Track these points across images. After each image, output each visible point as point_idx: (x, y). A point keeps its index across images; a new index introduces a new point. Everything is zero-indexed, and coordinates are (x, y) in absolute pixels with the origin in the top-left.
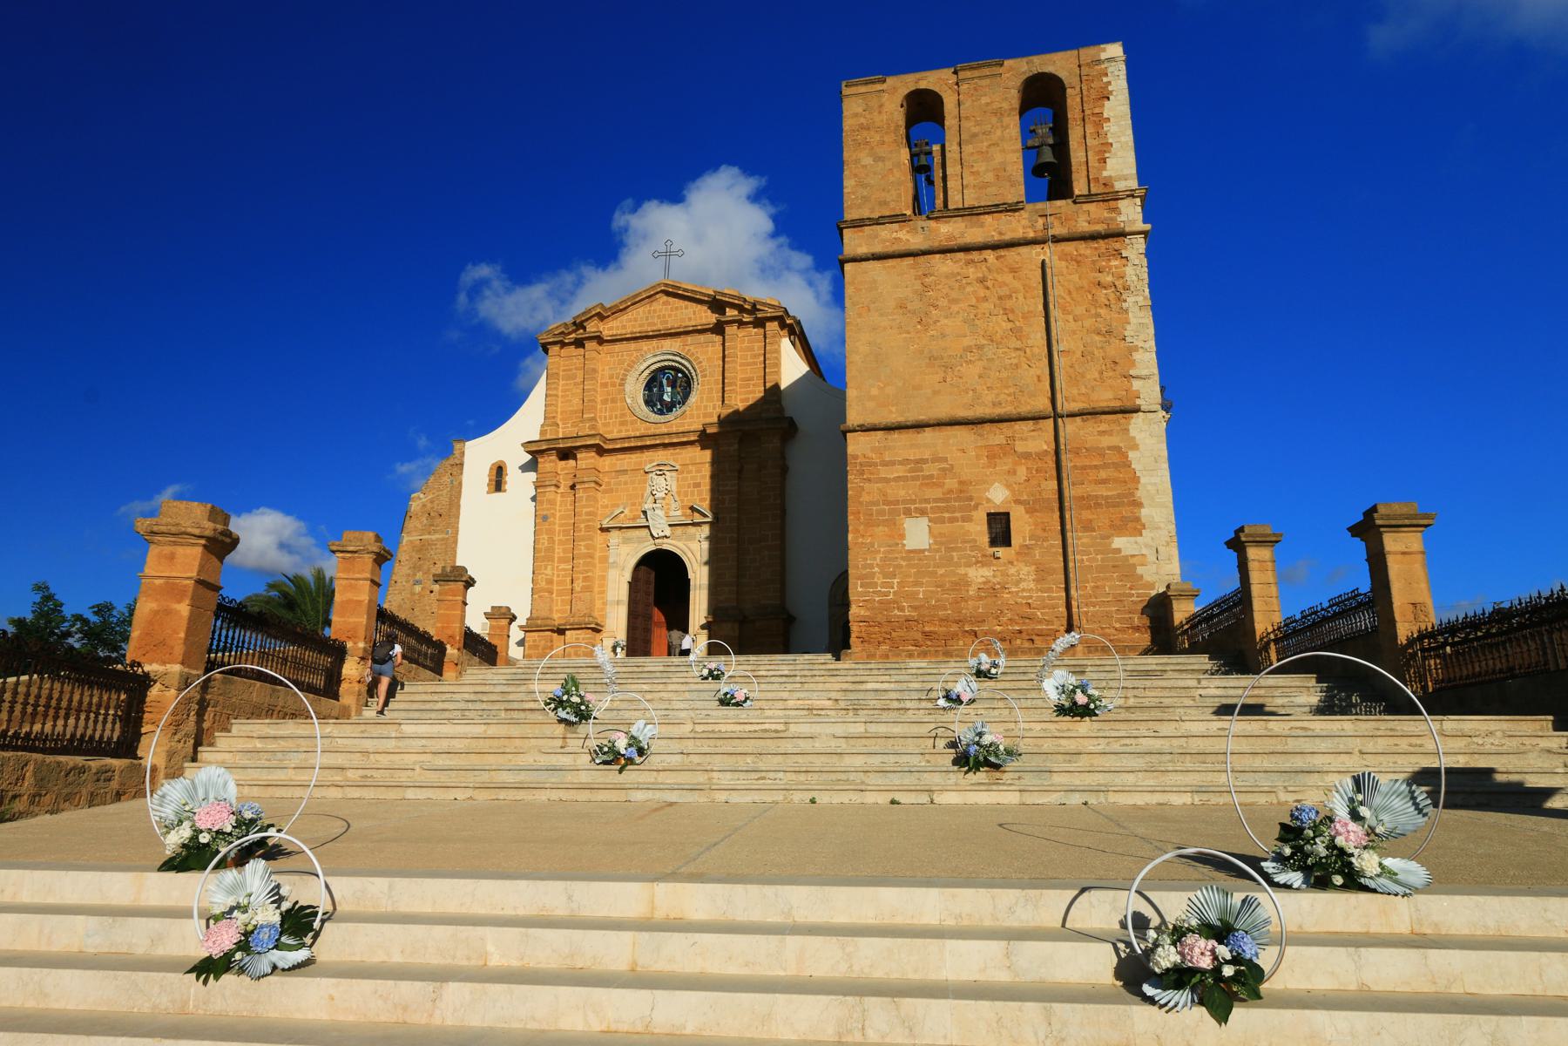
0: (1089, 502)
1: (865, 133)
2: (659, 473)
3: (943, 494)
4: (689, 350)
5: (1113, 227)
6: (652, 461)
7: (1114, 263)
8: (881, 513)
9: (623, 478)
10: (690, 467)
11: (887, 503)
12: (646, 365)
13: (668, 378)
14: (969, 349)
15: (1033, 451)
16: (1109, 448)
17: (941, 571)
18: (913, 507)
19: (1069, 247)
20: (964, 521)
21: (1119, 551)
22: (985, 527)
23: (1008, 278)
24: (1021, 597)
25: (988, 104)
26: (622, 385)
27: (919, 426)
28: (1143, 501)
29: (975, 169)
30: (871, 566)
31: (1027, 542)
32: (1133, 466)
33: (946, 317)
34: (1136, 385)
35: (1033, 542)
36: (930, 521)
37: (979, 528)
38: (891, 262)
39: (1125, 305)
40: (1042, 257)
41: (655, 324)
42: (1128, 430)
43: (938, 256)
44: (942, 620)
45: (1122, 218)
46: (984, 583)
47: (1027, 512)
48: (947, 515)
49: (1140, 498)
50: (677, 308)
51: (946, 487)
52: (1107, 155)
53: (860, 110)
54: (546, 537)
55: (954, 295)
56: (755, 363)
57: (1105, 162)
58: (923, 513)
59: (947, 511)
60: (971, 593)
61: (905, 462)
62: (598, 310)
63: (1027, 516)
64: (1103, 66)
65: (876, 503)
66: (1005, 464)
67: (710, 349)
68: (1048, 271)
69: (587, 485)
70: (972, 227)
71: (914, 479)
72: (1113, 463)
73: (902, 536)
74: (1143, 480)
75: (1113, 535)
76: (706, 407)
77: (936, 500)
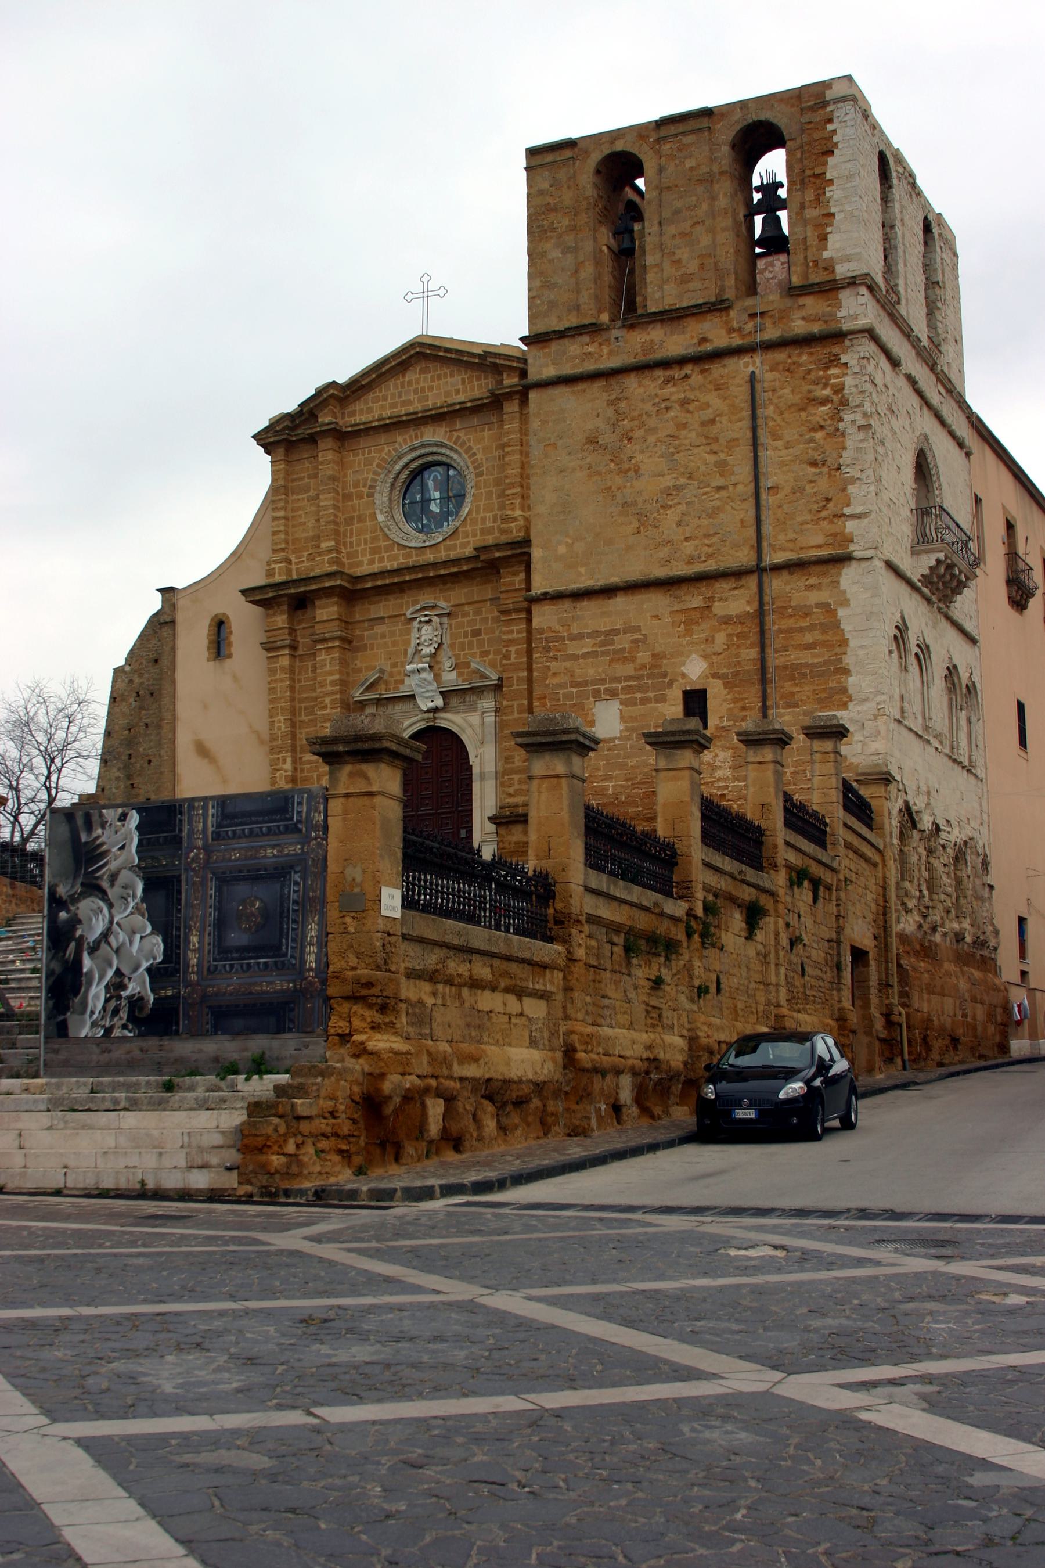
0: (794, 672)
1: (552, 216)
2: (423, 619)
4: (459, 437)
5: (833, 327)
6: (416, 602)
7: (833, 371)
8: (568, 696)
9: (379, 629)
10: (467, 608)
11: (574, 684)
12: (402, 463)
13: (435, 476)
16: (817, 606)
17: (631, 762)
18: (602, 688)
19: (780, 356)
20: (657, 701)
25: (692, 169)
26: (371, 495)
27: (608, 591)
28: (851, 668)
29: (677, 257)
31: (725, 724)
32: (842, 627)
33: (642, 452)
34: (851, 526)
35: (731, 723)
36: (621, 704)
38: (581, 386)
39: (841, 425)
40: (751, 369)
41: (409, 402)
42: (838, 583)
43: (633, 375)
45: (843, 313)
47: (725, 688)
48: (639, 695)
49: (848, 664)
50: (439, 378)
51: (639, 661)
52: (829, 230)
53: (546, 185)
54: (282, 718)
55: (652, 422)
58: (613, 694)
59: (639, 691)
61: (596, 633)
62: (331, 391)
63: (725, 692)
64: (829, 109)
65: (562, 686)
66: (700, 633)
67: (486, 433)
68: (758, 387)
69: (330, 645)
71: (605, 653)
72: (821, 624)
76: (484, 519)
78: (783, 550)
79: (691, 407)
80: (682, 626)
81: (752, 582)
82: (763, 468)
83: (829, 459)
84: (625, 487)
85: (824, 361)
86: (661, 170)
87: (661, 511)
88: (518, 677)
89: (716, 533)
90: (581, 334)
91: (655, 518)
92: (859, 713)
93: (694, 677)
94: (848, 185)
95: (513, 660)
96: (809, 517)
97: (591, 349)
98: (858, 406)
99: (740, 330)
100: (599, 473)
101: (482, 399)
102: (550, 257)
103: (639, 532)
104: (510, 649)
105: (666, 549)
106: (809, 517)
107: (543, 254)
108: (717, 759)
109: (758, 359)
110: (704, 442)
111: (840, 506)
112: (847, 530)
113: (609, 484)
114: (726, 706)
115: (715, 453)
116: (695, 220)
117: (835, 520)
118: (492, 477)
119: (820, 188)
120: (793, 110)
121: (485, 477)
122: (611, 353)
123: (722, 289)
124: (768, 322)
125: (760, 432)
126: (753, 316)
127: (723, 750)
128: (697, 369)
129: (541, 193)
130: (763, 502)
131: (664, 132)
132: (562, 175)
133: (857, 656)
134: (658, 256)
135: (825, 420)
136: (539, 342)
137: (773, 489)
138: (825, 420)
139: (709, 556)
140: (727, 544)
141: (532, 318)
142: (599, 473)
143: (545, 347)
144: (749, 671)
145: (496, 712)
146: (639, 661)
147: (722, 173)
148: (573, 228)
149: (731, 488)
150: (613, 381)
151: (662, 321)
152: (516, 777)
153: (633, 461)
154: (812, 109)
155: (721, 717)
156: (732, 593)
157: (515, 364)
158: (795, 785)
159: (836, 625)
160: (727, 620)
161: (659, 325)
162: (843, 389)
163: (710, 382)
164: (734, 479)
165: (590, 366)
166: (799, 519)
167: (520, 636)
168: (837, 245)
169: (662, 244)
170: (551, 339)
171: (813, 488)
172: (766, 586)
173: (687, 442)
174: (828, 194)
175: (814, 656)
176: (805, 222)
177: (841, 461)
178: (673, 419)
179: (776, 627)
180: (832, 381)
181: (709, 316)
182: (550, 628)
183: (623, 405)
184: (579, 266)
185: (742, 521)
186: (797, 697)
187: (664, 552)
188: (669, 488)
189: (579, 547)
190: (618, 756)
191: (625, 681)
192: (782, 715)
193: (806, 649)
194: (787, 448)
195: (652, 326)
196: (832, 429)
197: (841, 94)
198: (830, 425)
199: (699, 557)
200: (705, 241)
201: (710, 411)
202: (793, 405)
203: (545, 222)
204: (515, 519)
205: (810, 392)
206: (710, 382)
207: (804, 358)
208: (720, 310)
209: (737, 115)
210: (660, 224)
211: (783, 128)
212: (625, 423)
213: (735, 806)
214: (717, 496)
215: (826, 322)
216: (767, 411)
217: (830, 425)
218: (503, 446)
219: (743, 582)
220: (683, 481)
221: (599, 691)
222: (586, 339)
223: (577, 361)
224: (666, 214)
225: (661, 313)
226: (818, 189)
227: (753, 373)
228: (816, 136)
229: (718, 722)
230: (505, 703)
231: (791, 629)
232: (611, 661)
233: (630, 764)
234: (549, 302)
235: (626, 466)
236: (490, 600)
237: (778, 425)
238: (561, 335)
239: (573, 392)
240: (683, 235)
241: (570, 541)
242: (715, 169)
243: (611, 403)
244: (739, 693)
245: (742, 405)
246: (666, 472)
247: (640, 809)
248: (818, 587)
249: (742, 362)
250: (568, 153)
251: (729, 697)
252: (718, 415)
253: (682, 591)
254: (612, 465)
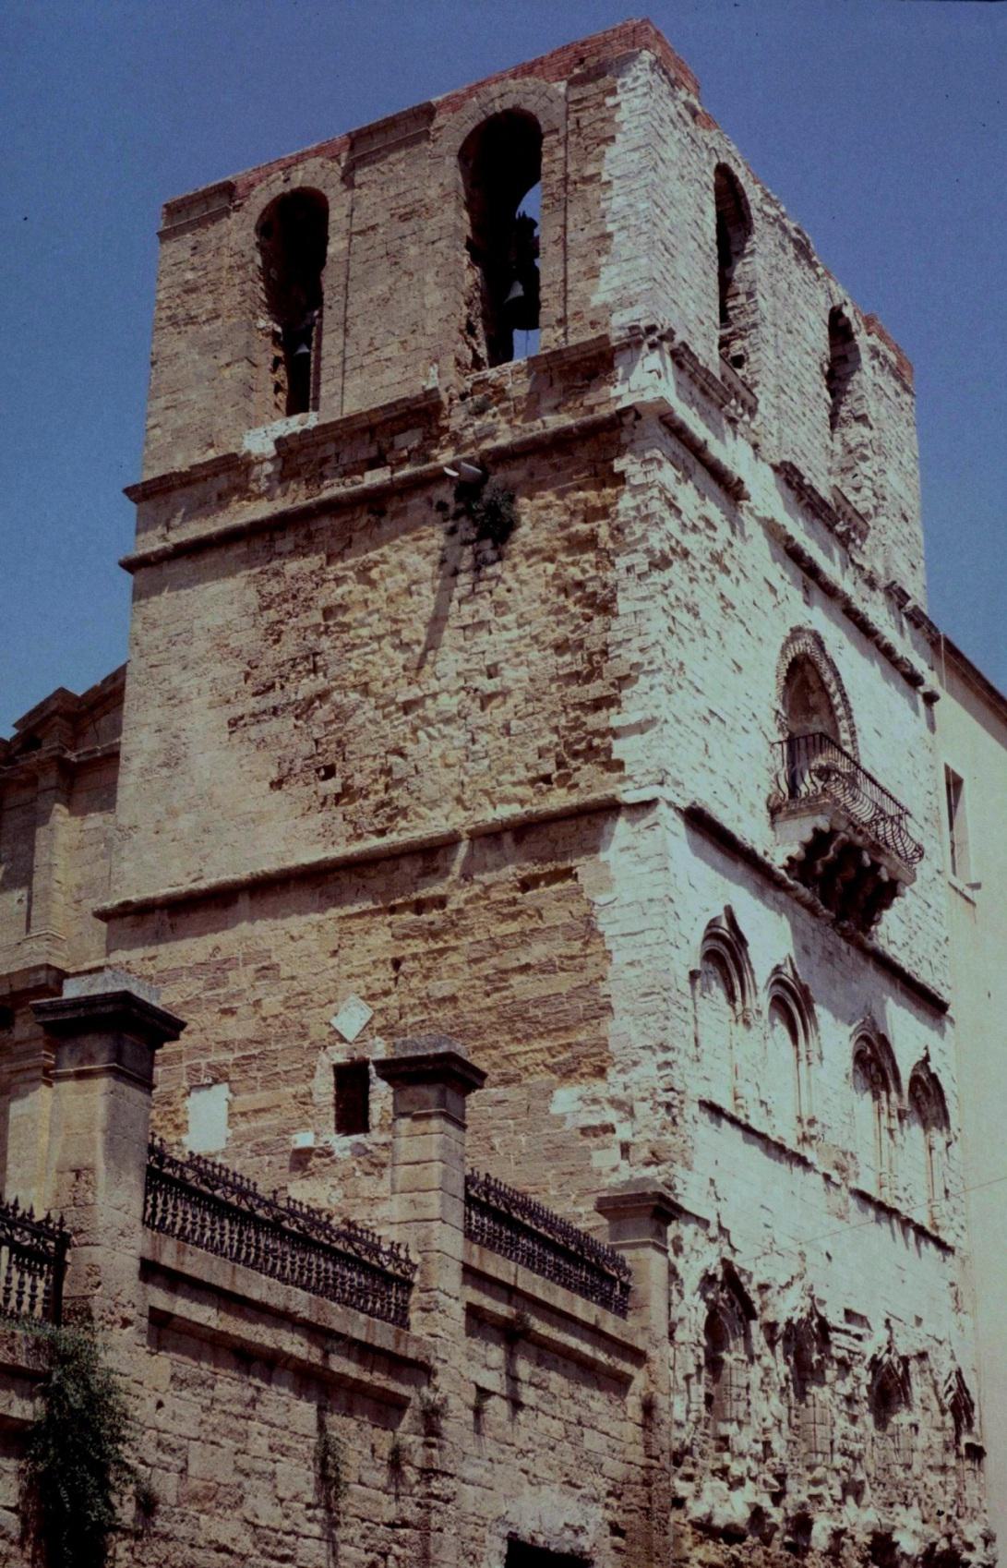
74: (618, 958)
194: (520, 626)
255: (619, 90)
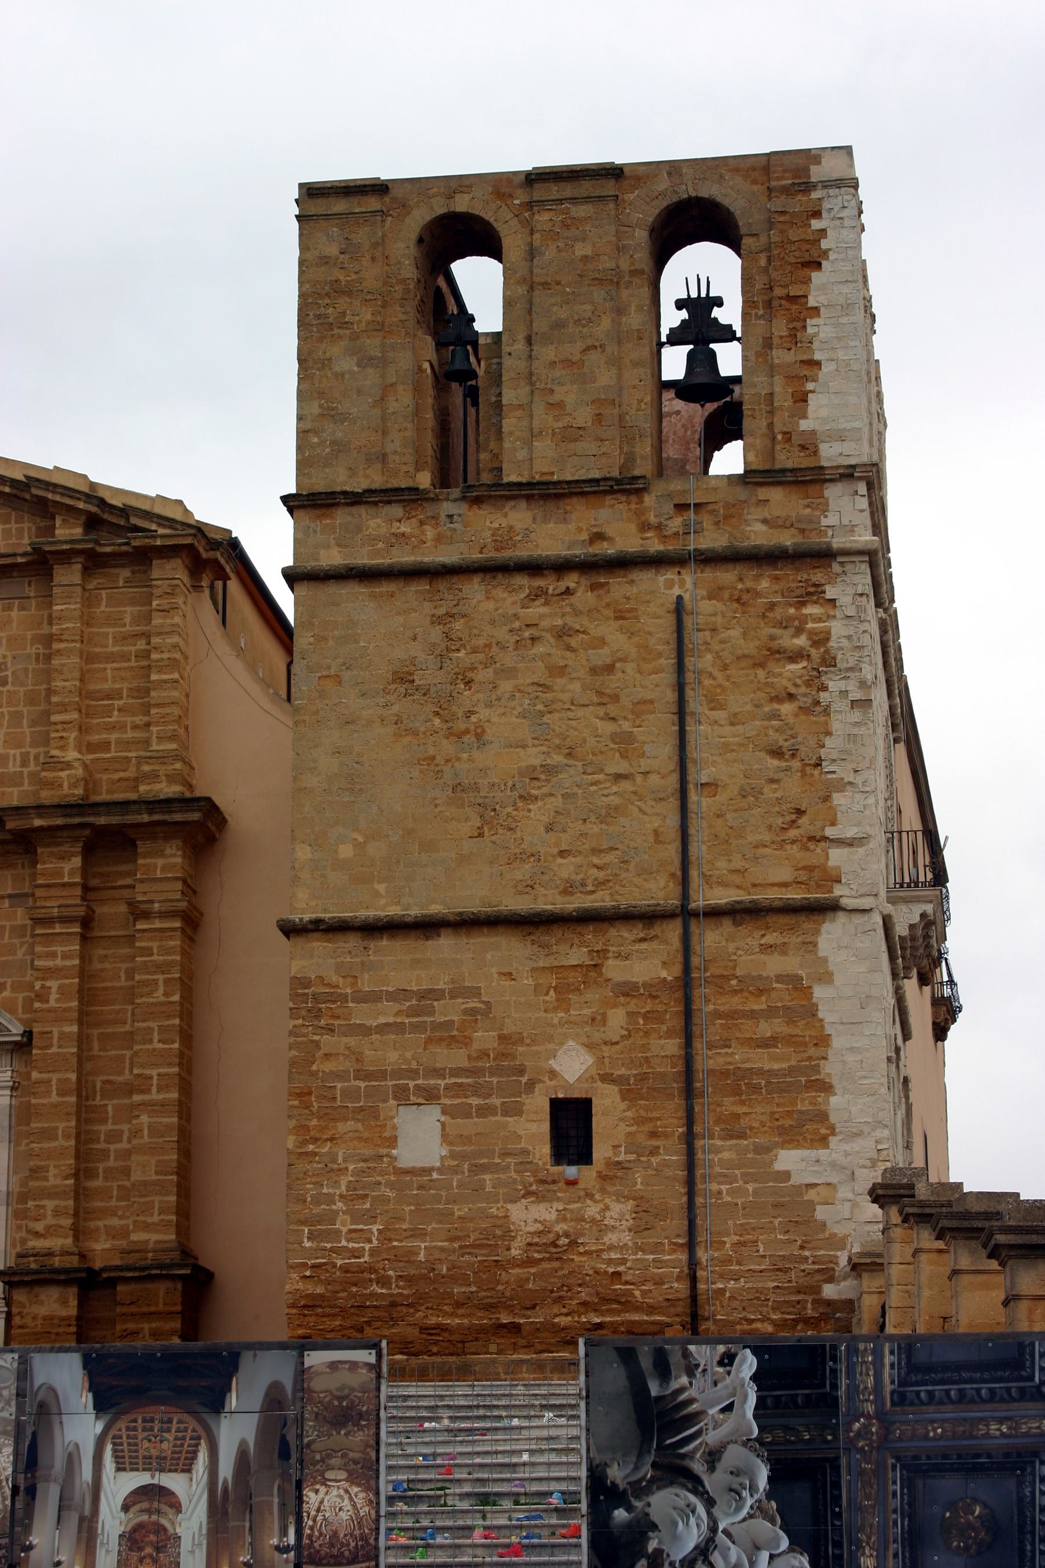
1: (343, 302)
3: (470, 1058)
5: (814, 540)
7: (811, 610)
8: (351, 1094)
11: (360, 1075)
14: (532, 775)
15: (640, 980)
16: (780, 978)
17: (460, 1210)
18: (411, 1084)
19: (727, 576)
20: (506, 1113)
21: (786, 1175)
22: (546, 1127)
23: (610, 631)
24: (604, 1261)
25: (585, 259)
28: (835, 1081)
29: (556, 398)
30: (330, 1199)
31: (622, 1157)
32: (820, 1015)
33: (489, 705)
34: (836, 856)
35: (633, 1157)
37: (533, 1127)
38: (385, 587)
39: (824, 696)
40: (676, 591)
42: (815, 945)
43: (477, 579)
44: (458, 1305)
45: (831, 520)
46: (539, 1233)
47: (623, 1099)
48: (475, 1101)
49: (829, 1075)
51: (476, 1046)
52: (810, 386)
53: (333, 250)
55: (508, 659)
56: (124, 657)
57: (806, 401)
58: (430, 1096)
59: (476, 1094)
60: (514, 1252)
61: (400, 995)
63: (623, 1106)
64: (814, 195)
66: (583, 1005)
67: (15, 614)
68: (688, 622)
70: (546, 520)
71: (416, 1028)
73: (392, 1142)
74: (837, 1043)
75: (776, 1145)
77: (456, 1072)
78: (725, 885)
79: (574, 642)
80: (552, 993)
81: (673, 931)
82: (692, 753)
83: (802, 748)
84: (458, 759)
85: (798, 592)
86: (532, 253)
87: (520, 804)
88: (62, 1035)
89: (612, 849)
90: (389, 502)
91: (508, 815)
92: (846, 1154)
93: (571, 1079)
94: (844, 320)
95: (52, 1003)
96: (767, 837)
97: (405, 528)
98: (851, 669)
99: (659, 527)
100: (415, 733)
101: (15, 555)
102: (337, 369)
103: (481, 835)
104: (48, 984)
105: (526, 866)
106: (767, 837)
107: (326, 363)
108: (608, 1214)
109: (688, 577)
110: (595, 699)
111: (819, 824)
112: (830, 863)
113: (431, 751)
114: (623, 1129)
115: (613, 719)
116: (590, 342)
117: (811, 845)
118: (22, 689)
119: (798, 319)
120: (755, 188)
121: (9, 687)
122: (439, 539)
123: (630, 459)
124: (707, 521)
125: (689, 693)
126: (682, 508)
127: (618, 1201)
128: (585, 582)
129: (325, 261)
130: (692, 807)
131: (540, 192)
132: (362, 236)
133: (844, 1062)
134: (524, 391)
135: (796, 685)
136: (315, 506)
137: (710, 787)
138: (796, 685)
139: (600, 884)
140: (632, 867)
141: (303, 465)
142: (415, 733)
143: (325, 516)
144: (663, 1076)
145: (13, 1088)
146: (476, 1046)
147: (634, 273)
148: (379, 327)
149: (639, 779)
150: (442, 585)
151: (529, 498)
152: (50, 1204)
153: (474, 719)
154: (786, 191)
155: (616, 1147)
156: (637, 947)
157: (81, 505)
158: (739, 1263)
159: (811, 1012)
160: (628, 990)
161: (523, 504)
162: (828, 639)
163: (608, 605)
164: (644, 764)
165: (403, 557)
166: (752, 838)
167: (68, 963)
168: (824, 413)
169: (531, 374)
170: (337, 505)
171: (776, 790)
172: (694, 939)
173: (566, 697)
174: (810, 330)
175: (773, 1058)
176: (772, 370)
177: (823, 752)
178: (542, 657)
179: (711, 1007)
180: (810, 625)
181: (608, 500)
182: (321, 978)
183: (458, 625)
184: (387, 389)
185: (656, 832)
186: (744, 1122)
187: (523, 871)
188: (534, 768)
189: (376, 850)
190: (437, 1199)
191: (452, 1076)
192: (718, 1150)
193: (759, 1047)
194: (732, 724)
195: (511, 503)
196: (810, 701)
197: (835, 176)
198: (805, 695)
199: (584, 885)
200: (605, 377)
201: (606, 651)
202: (744, 656)
203: (331, 310)
204: (68, 765)
205: (772, 638)
206: (608, 605)
207: (764, 584)
208: (628, 492)
209: (663, 184)
210: (529, 340)
211: (737, 213)
212: (462, 654)
213: (637, 1293)
214: (615, 789)
215: (802, 531)
216: (701, 662)
217: (805, 695)
218: (48, 640)
219: (657, 930)
220: (557, 758)
221: (405, 1088)
222: (397, 510)
223: (381, 545)
224: (540, 325)
225: (530, 485)
226: (793, 320)
227: (680, 598)
228: (794, 235)
229: (610, 1154)
230: (35, 1075)
231: (736, 1012)
232: (429, 1041)
233: (457, 1213)
234: (334, 443)
235: (461, 726)
236: (10, 896)
237: (720, 686)
238: (355, 499)
239: (373, 596)
240: (568, 363)
241: (361, 839)
242: (625, 265)
243: (437, 620)
244: (646, 1109)
245: (660, 648)
246: (530, 742)
247: (474, 1289)
248: (782, 949)
249: (661, 579)
250: (373, 203)
251: (629, 1114)
252: (620, 660)
253: (553, 937)
254: (437, 721)
255: (824, 214)
